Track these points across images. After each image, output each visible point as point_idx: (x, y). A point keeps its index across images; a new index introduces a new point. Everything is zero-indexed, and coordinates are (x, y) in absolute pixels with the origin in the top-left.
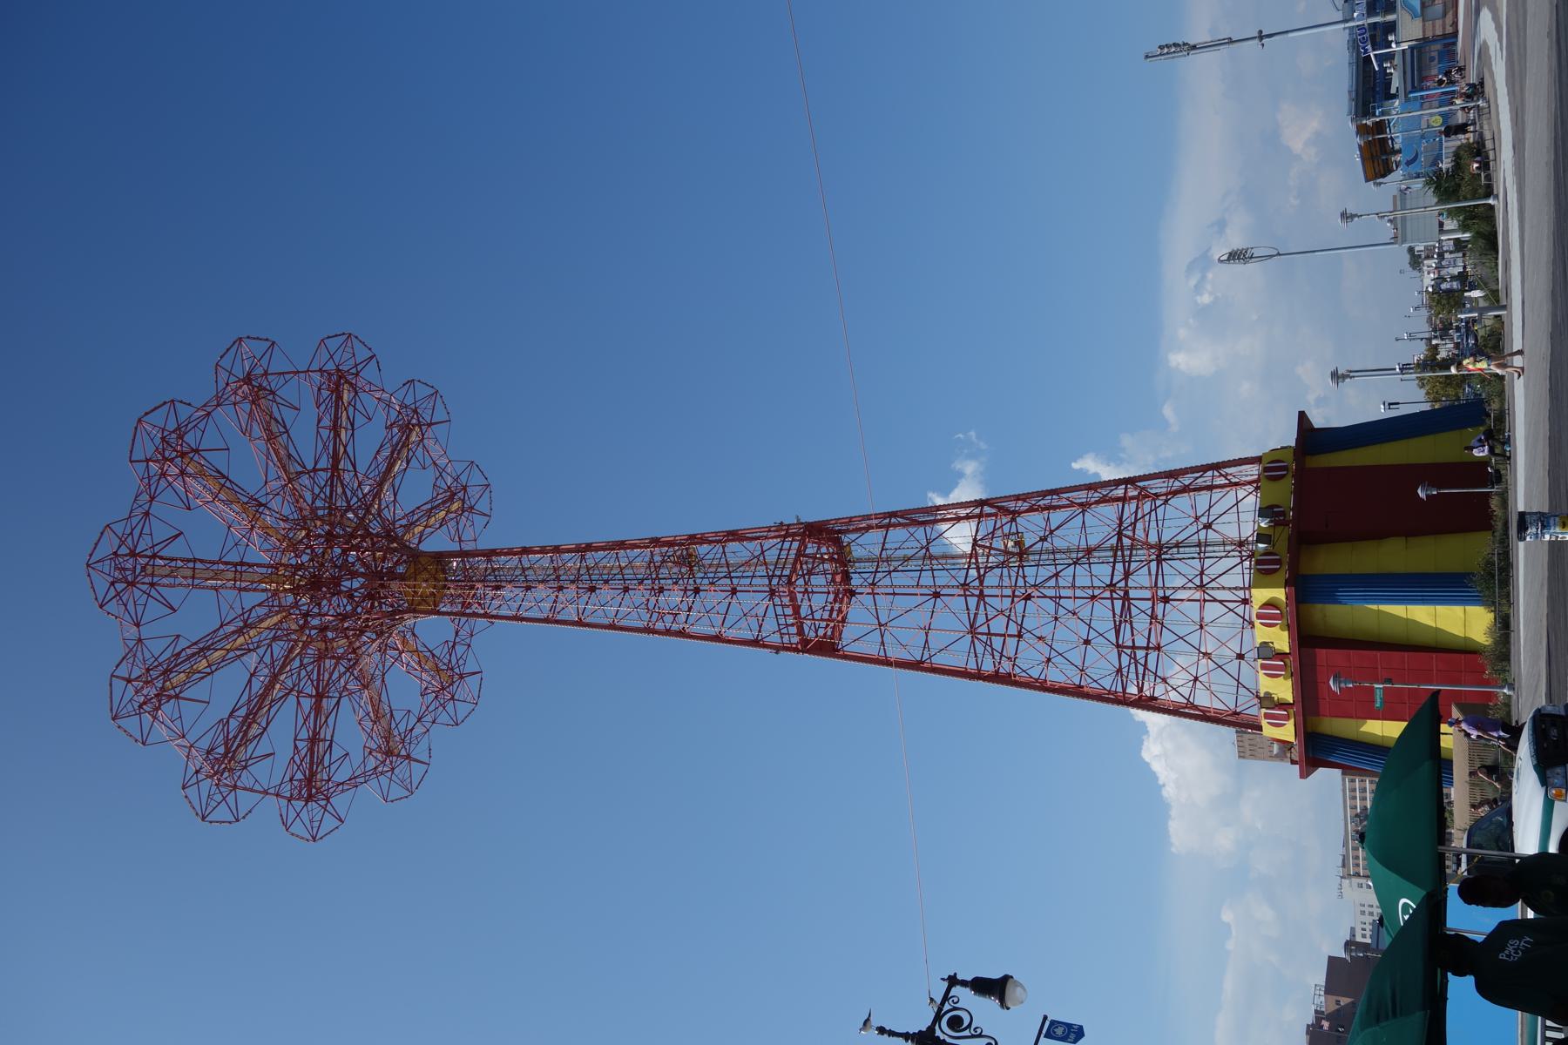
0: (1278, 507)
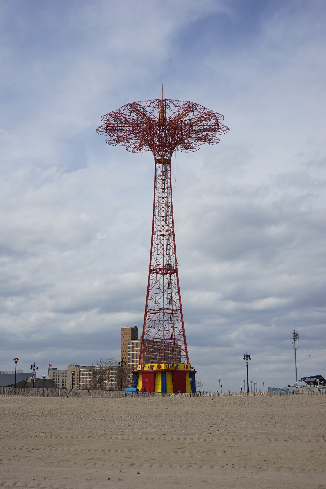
0: (179, 368)
